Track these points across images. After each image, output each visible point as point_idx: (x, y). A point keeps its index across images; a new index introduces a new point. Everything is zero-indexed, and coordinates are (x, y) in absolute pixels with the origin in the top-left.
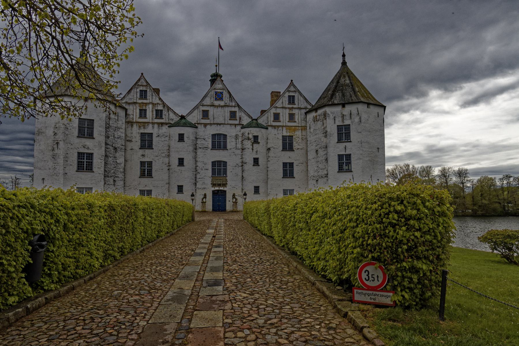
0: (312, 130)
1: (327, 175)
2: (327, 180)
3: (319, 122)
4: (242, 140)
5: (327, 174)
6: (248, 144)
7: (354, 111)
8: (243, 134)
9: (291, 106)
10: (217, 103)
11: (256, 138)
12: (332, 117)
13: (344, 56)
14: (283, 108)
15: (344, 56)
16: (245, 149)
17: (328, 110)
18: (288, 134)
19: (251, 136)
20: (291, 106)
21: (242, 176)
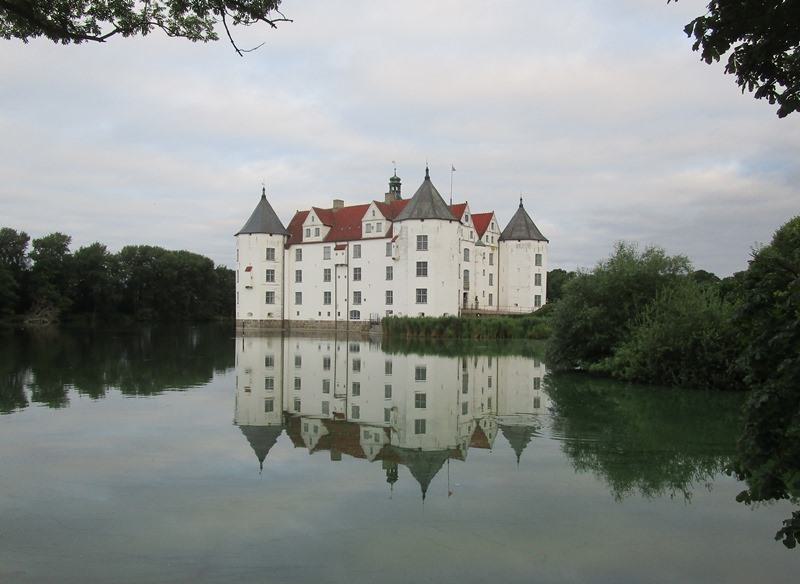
6: (480, 258)
10: (467, 224)
17: (532, 242)
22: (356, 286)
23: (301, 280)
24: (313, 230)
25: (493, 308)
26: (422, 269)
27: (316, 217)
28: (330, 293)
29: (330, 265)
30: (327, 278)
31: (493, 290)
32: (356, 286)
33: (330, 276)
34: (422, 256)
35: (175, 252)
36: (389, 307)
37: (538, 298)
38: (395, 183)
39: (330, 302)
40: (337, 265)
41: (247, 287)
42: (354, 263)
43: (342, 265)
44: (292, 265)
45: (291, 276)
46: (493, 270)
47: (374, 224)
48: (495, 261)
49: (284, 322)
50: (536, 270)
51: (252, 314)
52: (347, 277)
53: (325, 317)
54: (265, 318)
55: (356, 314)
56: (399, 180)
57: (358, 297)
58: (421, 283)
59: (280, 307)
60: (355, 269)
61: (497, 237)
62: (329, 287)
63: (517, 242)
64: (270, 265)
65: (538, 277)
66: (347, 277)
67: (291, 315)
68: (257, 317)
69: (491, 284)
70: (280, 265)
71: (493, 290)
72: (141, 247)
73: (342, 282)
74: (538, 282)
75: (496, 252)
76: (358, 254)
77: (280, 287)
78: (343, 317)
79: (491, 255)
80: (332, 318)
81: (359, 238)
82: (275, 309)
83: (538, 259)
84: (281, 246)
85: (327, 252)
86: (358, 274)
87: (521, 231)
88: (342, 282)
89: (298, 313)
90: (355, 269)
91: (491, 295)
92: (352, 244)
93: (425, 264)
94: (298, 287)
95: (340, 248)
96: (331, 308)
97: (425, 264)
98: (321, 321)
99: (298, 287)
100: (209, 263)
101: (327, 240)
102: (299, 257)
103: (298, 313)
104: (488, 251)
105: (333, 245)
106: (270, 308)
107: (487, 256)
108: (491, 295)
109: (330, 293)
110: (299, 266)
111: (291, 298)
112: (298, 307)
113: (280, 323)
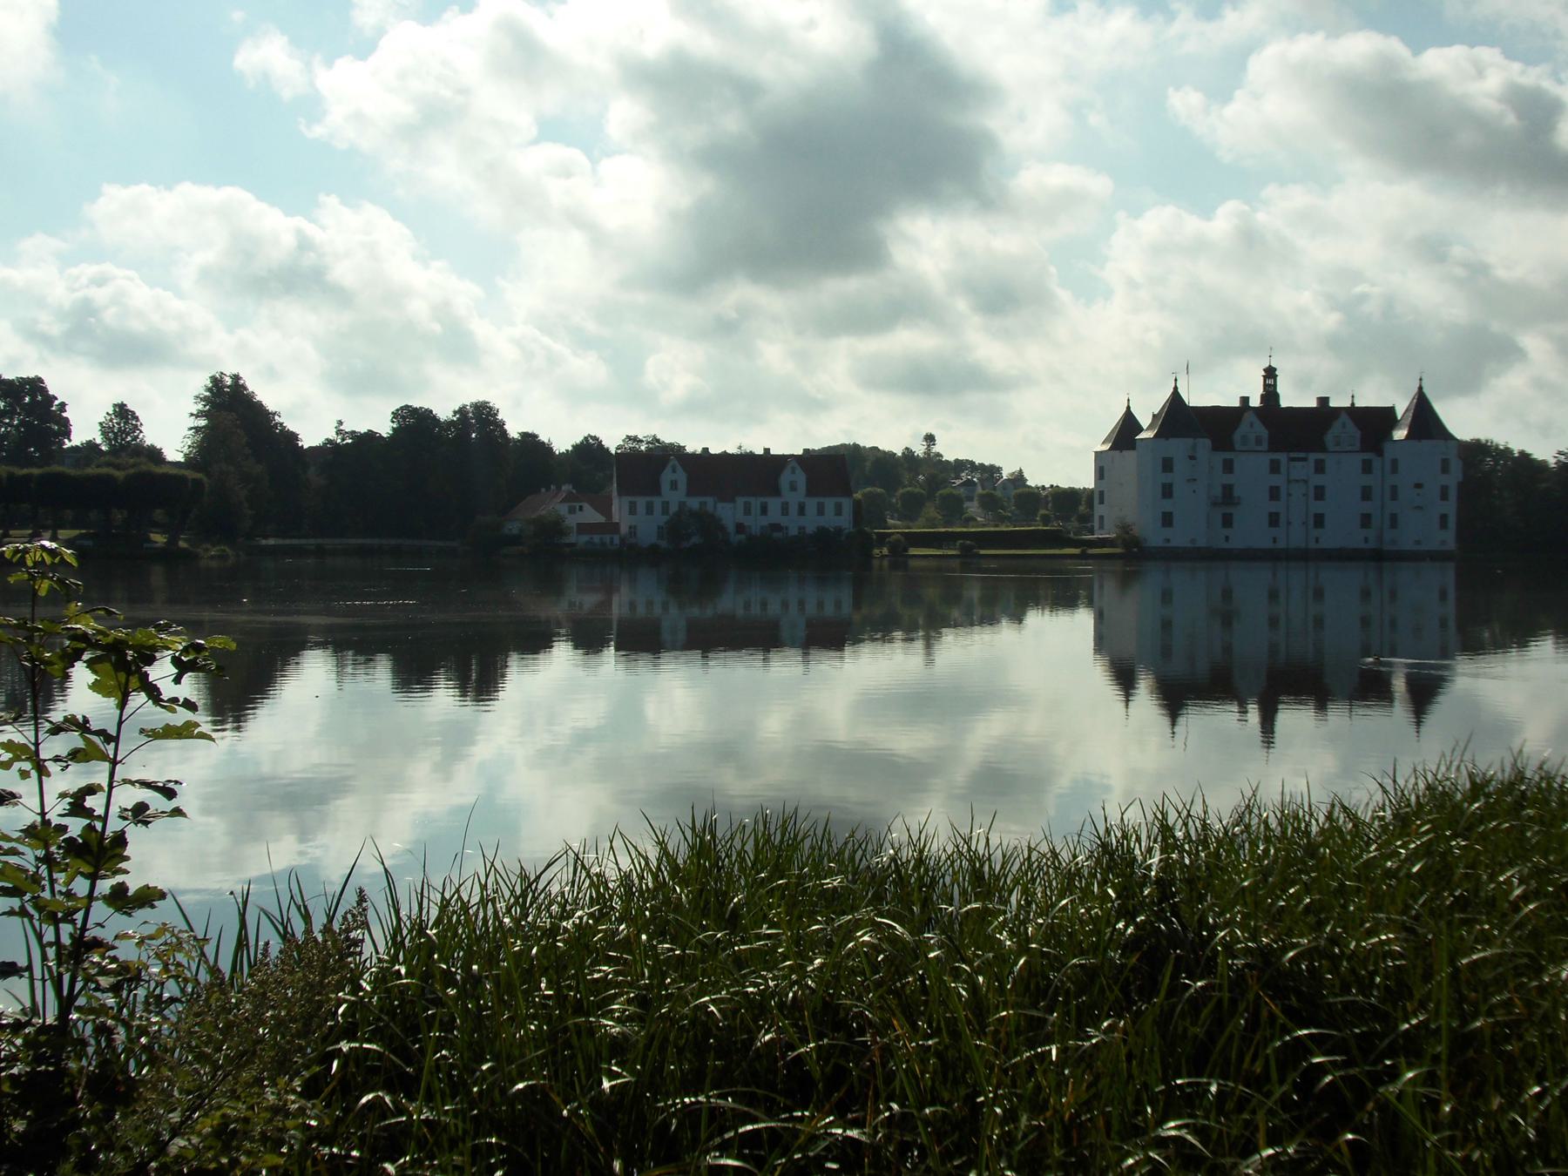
22: (1317, 507)
30: (1274, 493)
32: (1317, 507)
42: (1318, 480)
43: (1297, 481)
56: (1275, 369)
57: (1319, 521)
60: (1316, 488)
62: (1274, 507)
76: (1320, 468)
81: (1324, 449)
85: (1275, 467)
86: (1320, 493)
89: (1227, 538)
90: (1316, 488)
92: (1313, 457)
95: (1305, 459)
101: (1275, 446)
102: (1228, 467)
103: (1227, 538)
105: (1282, 457)
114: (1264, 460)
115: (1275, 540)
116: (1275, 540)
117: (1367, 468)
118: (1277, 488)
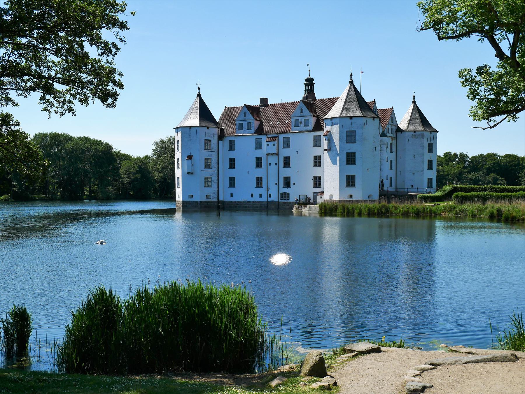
0: (410, 143)
1: (423, 171)
2: (423, 174)
3: (417, 139)
4: (381, 145)
5: (423, 170)
6: (384, 147)
7: (435, 137)
8: (381, 141)
9: (391, 123)
11: (387, 143)
12: (426, 138)
13: (414, 97)
14: (390, 124)
15: (414, 97)
16: (383, 151)
18: (391, 142)
19: (386, 143)
20: (391, 123)
21: (381, 168)
22: (285, 172)
23: (234, 167)
24: (245, 123)
25: (392, 189)
26: (351, 159)
27: (248, 113)
28: (261, 178)
29: (260, 154)
30: (259, 163)
31: (392, 174)
32: (285, 172)
33: (261, 164)
34: (351, 148)
35: (79, 138)
36: (318, 190)
37: (430, 180)
38: (310, 83)
39: (261, 186)
40: (268, 155)
41: (188, 173)
42: (285, 153)
43: (272, 154)
44: (225, 155)
45: (224, 164)
46: (392, 157)
47: (303, 119)
48: (394, 149)
49: (219, 202)
50: (427, 157)
51: (192, 196)
52: (277, 164)
53: (257, 199)
54: (204, 199)
55: (286, 196)
56: (312, 80)
57: (287, 182)
58: (351, 170)
59: (216, 189)
61: (394, 128)
62: (260, 172)
63: (413, 133)
64: (207, 154)
65: (430, 163)
66: (277, 164)
67: (225, 197)
68: (197, 198)
69: (391, 169)
70: (215, 154)
71: (392, 174)
72: (51, 134)
73: (272, 169)
74: (430, 167)
75: (394, 142)
76: (287, 144)
77: (216, 173)
78: (274, 198)
79: (391, 144)
80: (264, 199)
82: (212, 191)
83: (431, 148)
84: (216, 137)
85: (259, 146)
86: (287, 162)
87: (415, 124)
88: (272, 169)
89: (232, 195)
91: (391, 178)
93: (354, 154)
94: (232, 173)
96: (262, 191)
97: (354, 154)
98: (254, 202)
99: (232, 173)
100: (109, 148)
103: (232, 195)
104: (388, 140)
105: (264, 138)
106: (209, 191)
107: (389, 146)
108: (391, 178)
109: (261, 178)
110: (232, 155)
111: (224, 182)
112: (232, 190)
113: (216, 204)
114: (251, 141)
115: (261, 196)
116: (261, 196)
117: (317, 143)
118: (261, 159)
